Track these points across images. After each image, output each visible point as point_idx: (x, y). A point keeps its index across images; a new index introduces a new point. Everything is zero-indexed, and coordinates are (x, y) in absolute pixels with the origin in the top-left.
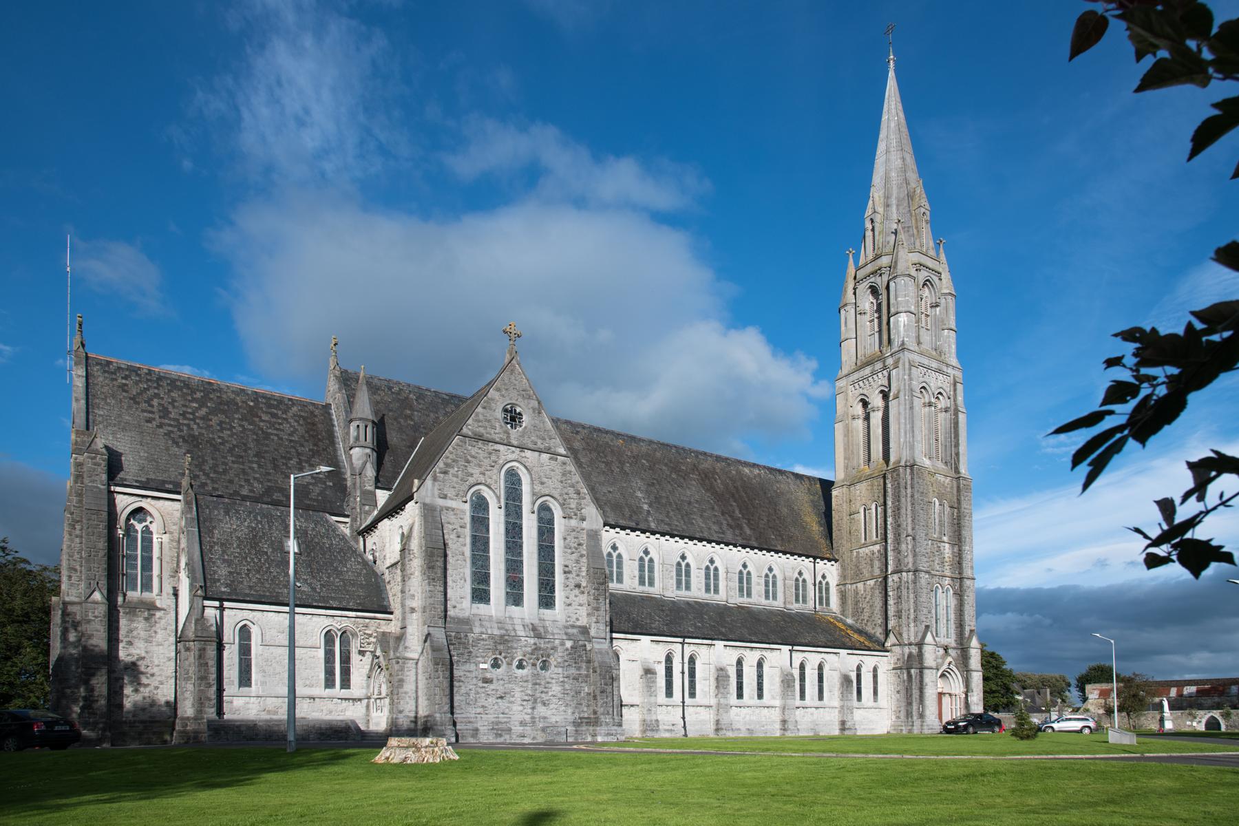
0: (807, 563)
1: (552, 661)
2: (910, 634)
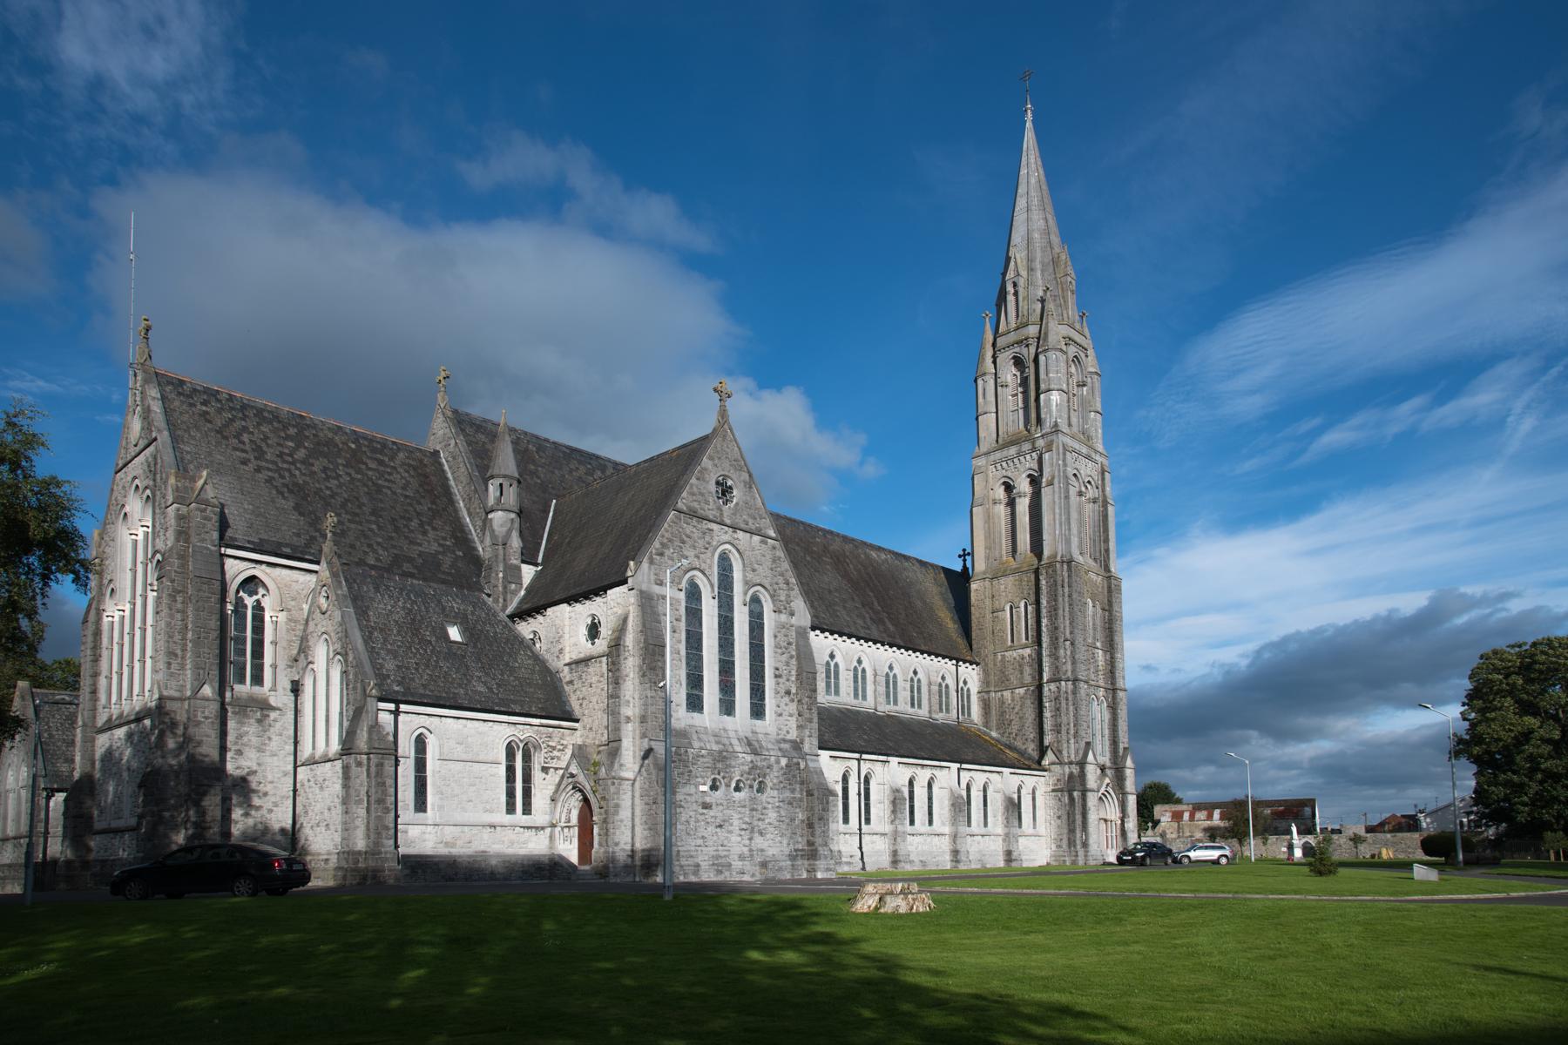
0: (948, 666)
2: (1071, 751)
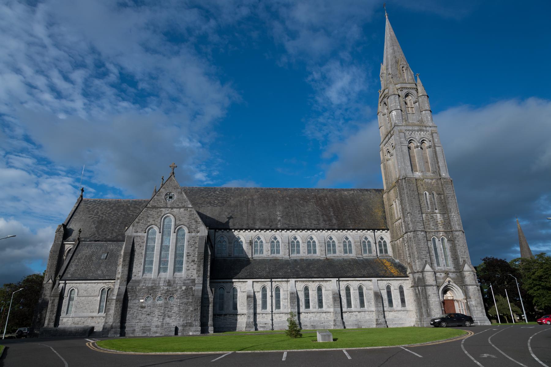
0: (369, 234)
1: (175, 296)
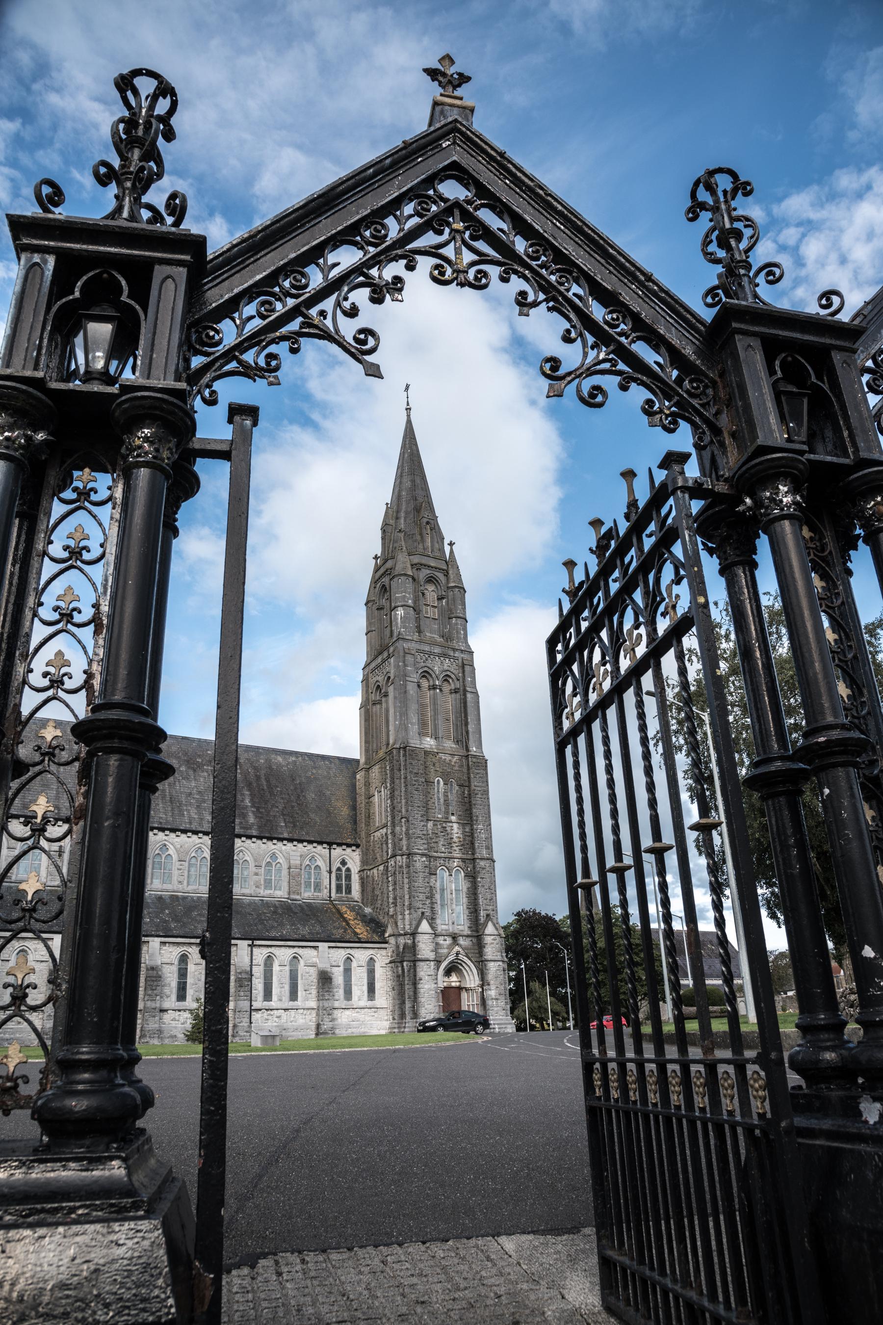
0: (321, 850)
